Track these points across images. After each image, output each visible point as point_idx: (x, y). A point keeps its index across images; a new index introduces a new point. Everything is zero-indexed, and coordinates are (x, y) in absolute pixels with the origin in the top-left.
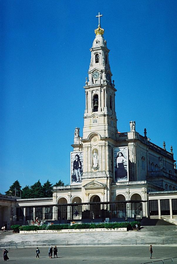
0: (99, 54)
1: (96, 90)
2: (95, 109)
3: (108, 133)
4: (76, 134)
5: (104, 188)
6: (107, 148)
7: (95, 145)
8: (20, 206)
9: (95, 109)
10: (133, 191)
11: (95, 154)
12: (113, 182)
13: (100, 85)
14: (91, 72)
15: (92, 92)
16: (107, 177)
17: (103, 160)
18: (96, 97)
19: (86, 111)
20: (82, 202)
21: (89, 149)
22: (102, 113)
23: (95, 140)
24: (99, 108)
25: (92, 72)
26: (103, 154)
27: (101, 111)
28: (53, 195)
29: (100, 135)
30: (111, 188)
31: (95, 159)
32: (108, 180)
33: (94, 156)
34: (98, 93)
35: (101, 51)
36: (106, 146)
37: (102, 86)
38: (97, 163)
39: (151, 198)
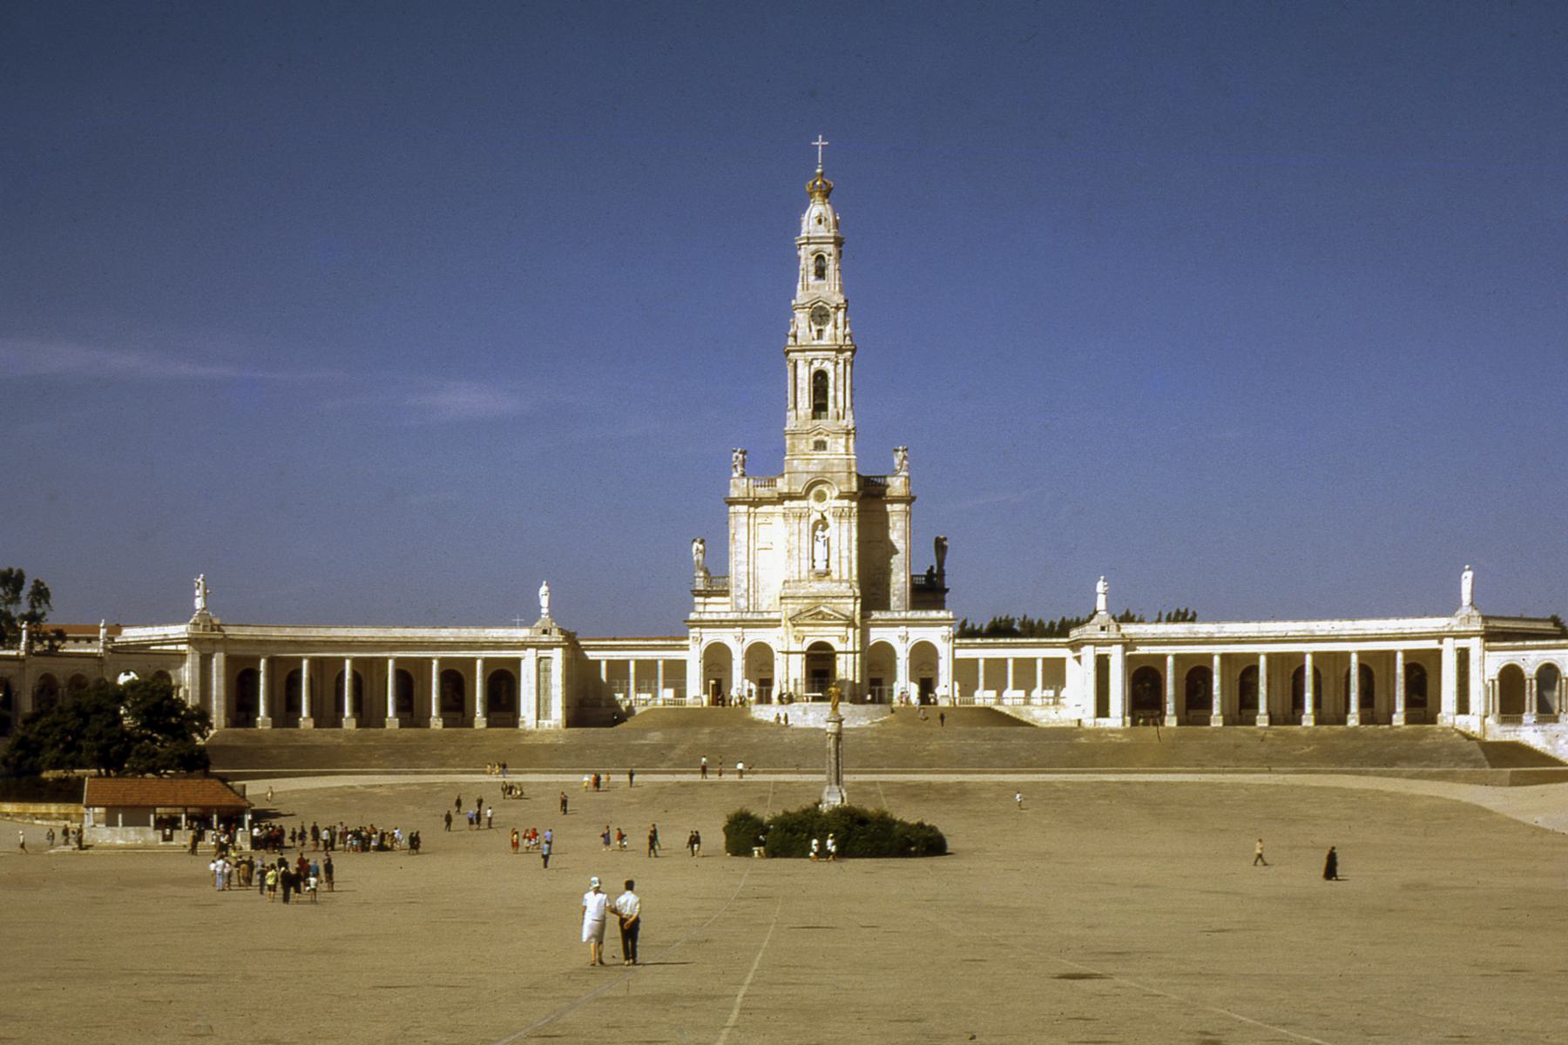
0: (827, 257)
4: (735, 466)
5: (848, 626)
8: (590, 658)
9: (819, 408)
10: (918, 634)
11: (819, 533)
12: (867, 608)
13: (837, 347)
14: (806, 306)
16: (856, 598)
18: (820, 379)
19: (791, 414)
20: (804, 656)
21: (804, 521)
23: (821, 497)
25: (809, 305)
27: (838, 418)
28: (691, 635)
30: (862, 623)
31: (819, 547)
32: (858, 606)
33: (817, 540)
34: (828, 367)
35: (831, 248)
37: (840, 350)
38: (826, 558)
39: (962, 654)
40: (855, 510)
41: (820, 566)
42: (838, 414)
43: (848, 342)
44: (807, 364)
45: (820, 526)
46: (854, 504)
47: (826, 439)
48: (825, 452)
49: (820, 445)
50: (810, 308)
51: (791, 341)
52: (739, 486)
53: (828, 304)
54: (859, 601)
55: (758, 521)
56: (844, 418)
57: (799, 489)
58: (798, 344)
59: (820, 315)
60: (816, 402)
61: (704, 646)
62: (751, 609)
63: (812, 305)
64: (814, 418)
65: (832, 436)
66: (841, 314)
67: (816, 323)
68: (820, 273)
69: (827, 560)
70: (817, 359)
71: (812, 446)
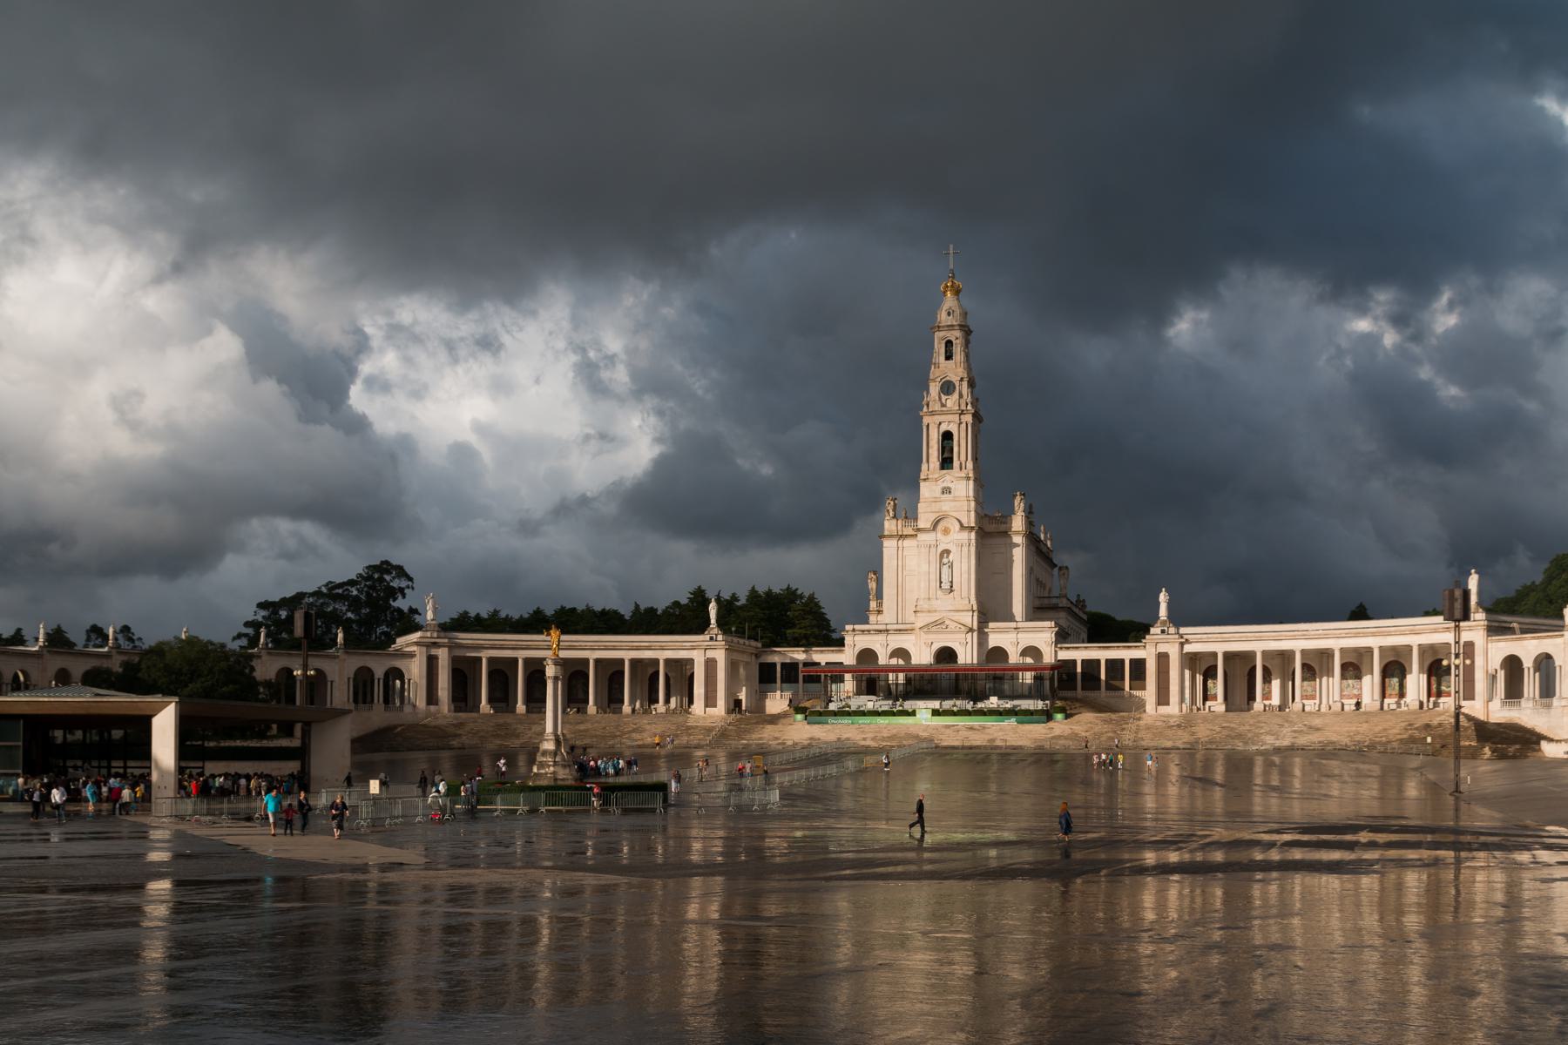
0: (954, 342)
2: (946, 463)
3: (976, 517)
6: (973, 549)
9: (946, 463)
10: (1027, 639)
11: (945, 561)
16: (973, 611)
17: (965, 576)
21: (933, 550)
23: (946, 531)
24: (956, 463)
27: (961, 469)
29: (957, 519)
31: (945, 569)
32: (975, 618)
34: (953, 428)
35: (958, 333)
40: (973, 542)
41: (946, 585)
47: (950, 485)
49: (946, 490)
51: (925, 409)
52: (890, 526)
57: (928, 525)
59: (947, 388)
60: (944, 456)
61: (857, 650)
62: (900, 621)
64: (942, 468)
67: (944, 394)
68: (949, 357)
69: (952, 582)
71: (940, 491)
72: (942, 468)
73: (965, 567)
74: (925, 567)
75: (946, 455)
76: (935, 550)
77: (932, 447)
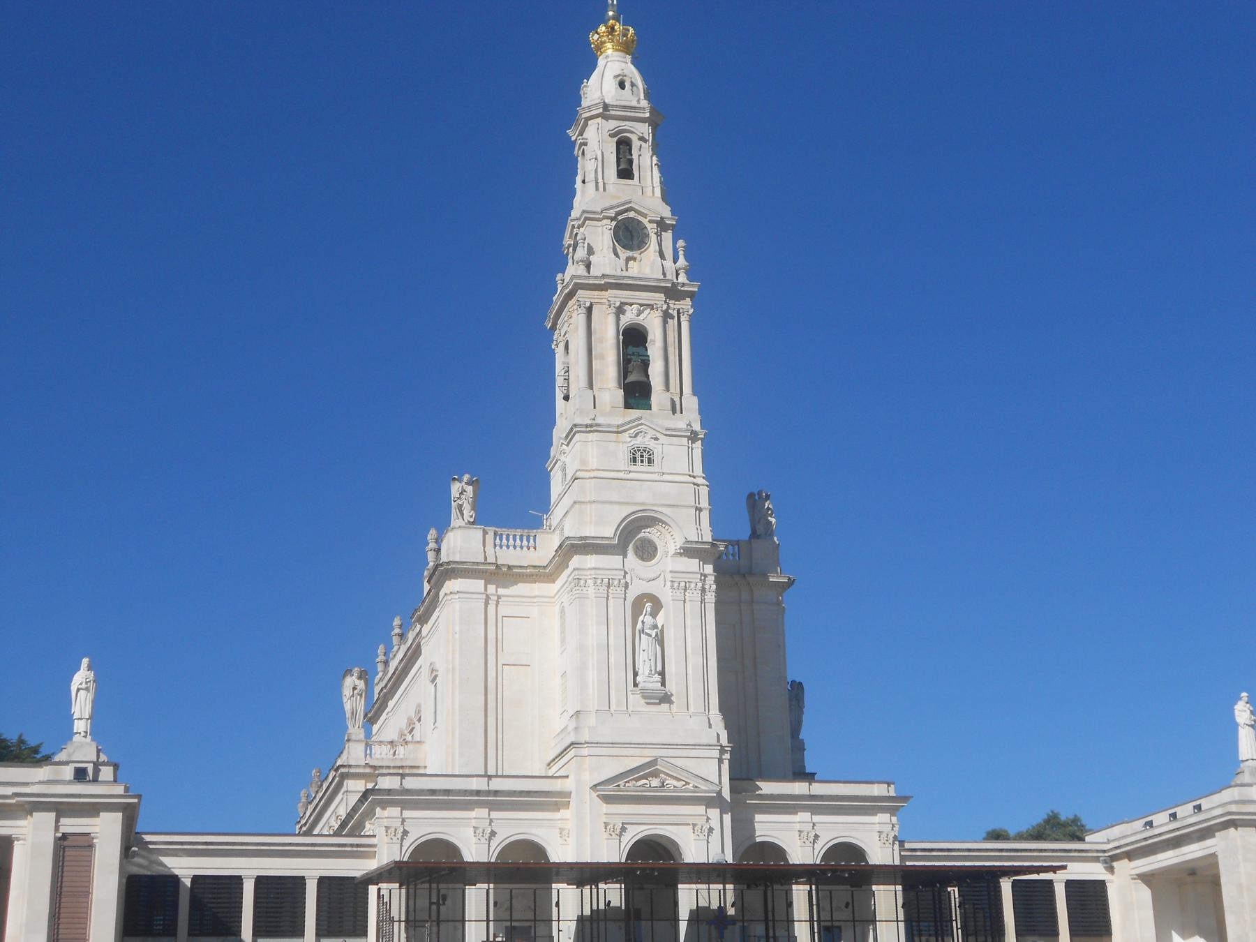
0: (636, 144)
1: (641, 305)
4: (460, 507)
6: (711, 597)
7: (653, 576)
15: (620, 311)
16: (722, 751)
17: (695, 660)
18: (634, 339)
21: (617, 591)
22: (680, 422)
24: (658, 396)
25: (612, 213)
26: (693, 622)
27: (674, 411)
32: (726, 766)
33: (642, 631)
34: (653, 324)
36: (707, 587)
37: (673, 293)
38: (659, 668)
40: (711, 580)
42: (673, 402)
43: (682, 278)
44: (612, 310)
45: (648, 606)
46: (709, 569)
47: (652, 445)
48: (650, 469)
49: (641, 456)
50: (612, 219)
53: (645, 216)
54: (727, 756)
55: (503, 610)
56: (682, 413)
58: (594, 272)
63: (618, 214)
64: (627, 405)
65: (662, 439)
66: (668, 236)
68: (625, 173)
69: (662, 674)
70: (631, 305)
71: (628, 456)
72: (627, 405)
73: (694, 641)
74: (594, 634)
75: (631, 378)
76: (621, 590)
77: (602, 357)
